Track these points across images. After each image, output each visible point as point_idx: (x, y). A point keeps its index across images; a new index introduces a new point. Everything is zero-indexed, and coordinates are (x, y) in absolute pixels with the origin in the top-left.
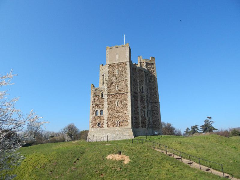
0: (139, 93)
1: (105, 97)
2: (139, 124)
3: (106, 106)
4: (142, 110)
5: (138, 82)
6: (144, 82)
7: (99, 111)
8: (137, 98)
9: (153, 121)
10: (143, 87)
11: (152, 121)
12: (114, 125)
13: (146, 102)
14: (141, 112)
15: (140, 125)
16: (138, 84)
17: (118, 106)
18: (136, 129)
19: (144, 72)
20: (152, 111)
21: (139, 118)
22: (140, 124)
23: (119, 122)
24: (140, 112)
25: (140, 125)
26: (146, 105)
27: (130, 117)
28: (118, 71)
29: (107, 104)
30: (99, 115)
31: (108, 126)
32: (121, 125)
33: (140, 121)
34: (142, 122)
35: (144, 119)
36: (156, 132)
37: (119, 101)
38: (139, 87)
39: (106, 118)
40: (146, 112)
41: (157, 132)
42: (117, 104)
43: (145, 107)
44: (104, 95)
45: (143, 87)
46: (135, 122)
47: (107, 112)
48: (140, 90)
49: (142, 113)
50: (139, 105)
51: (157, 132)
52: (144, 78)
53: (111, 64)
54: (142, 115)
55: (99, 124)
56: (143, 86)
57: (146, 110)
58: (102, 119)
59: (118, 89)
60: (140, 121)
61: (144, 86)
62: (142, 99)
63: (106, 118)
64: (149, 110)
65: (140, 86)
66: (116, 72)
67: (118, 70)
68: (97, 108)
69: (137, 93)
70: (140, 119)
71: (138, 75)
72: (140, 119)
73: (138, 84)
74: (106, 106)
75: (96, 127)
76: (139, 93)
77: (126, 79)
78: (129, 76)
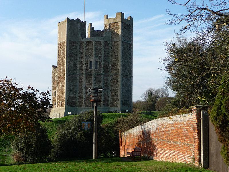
0: (84, 71)
5: (84, 57)
6: (93, 56)
9: (112, 98)
13: (93, 79)
15: (83, 104)
16: (84, 60)
22: (84, 103)
24: (84, 91)
25: (83, 104)
30: (55, 96)
33: (83, 100)
36: (69, 112)
38: (84, 63)
41: (70, 112)
45: (91, 62)
46: (79, 101)
48: (87, 66)
50: (84, 84)
51: (70, 112)
54: (86, 94)
56: (91, 60)
60: (83, 100)
65: (86, 62)
69: (82, 71)
70: (84, 97)
71: (85, 49)
72: (84, 97)
73: (84, 60)
76: (84, 71)
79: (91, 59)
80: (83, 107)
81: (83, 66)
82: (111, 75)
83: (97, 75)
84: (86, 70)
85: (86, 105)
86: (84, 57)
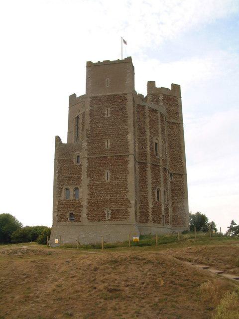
1: (85, 164)
2: (147, 216)
3: (85, 180)
4: (154, 188)
5: (148, 133)
6: (160, 135)
7: (72, 189)
8: (145, 164)
10: (156, 144)
11: (171, 210)
12: (101, 218)
13: (162, 174)
14: (153, 192)
15: (151, 217)
16: (148, 137)
17: (109, 181)
18: (142, 225)
19: (159, 115)
20: (172, 190)
21: (147, 204)
23: (110, 213)
24: (150, 193)
26: (162, 180)
27: (133, 202)
28: (109, 112)
29: (87, 178)
30: (71, 198)
31: (90, 217)
32: (115, 218)
33: (150, 211)
34: (153, 212)
35: (157, 207)
37: (112, 171)
39: (84, 203)
40: (162, 193)
42: (107, 177)
43: (160, 183)
44: (80, 160)
46: (140, 212)
47: (87, 191)
48: (152, 149)
49: (153, 195)
52: (159, 126)
53: (94, 97)
55: (71, 214)
56: (157, 141)
57: (162, 189)
58: (77, 205)
59: (109, 147)
60: (150, 211)
61: (160, 142)
62: (155, 166)
63: (84, 203)
64: (167, 189)
65: (151, 142)
66: (106, 112)
67: (109, 109)
68: (68, 184)
70: (151, 206)
71: (148, 119)
72: (151, 206)
73: (148, 137)
74: (85, 180)
75: (66, 220)
77: (126, 127)
78: (130, 121)
79: (157, 139)
80: (151, 224)
81: (146, 148)
82: (171, 174)
83: (164, 168)
84: (152, 155)
85: (155, 222)
86: (148, 133)
